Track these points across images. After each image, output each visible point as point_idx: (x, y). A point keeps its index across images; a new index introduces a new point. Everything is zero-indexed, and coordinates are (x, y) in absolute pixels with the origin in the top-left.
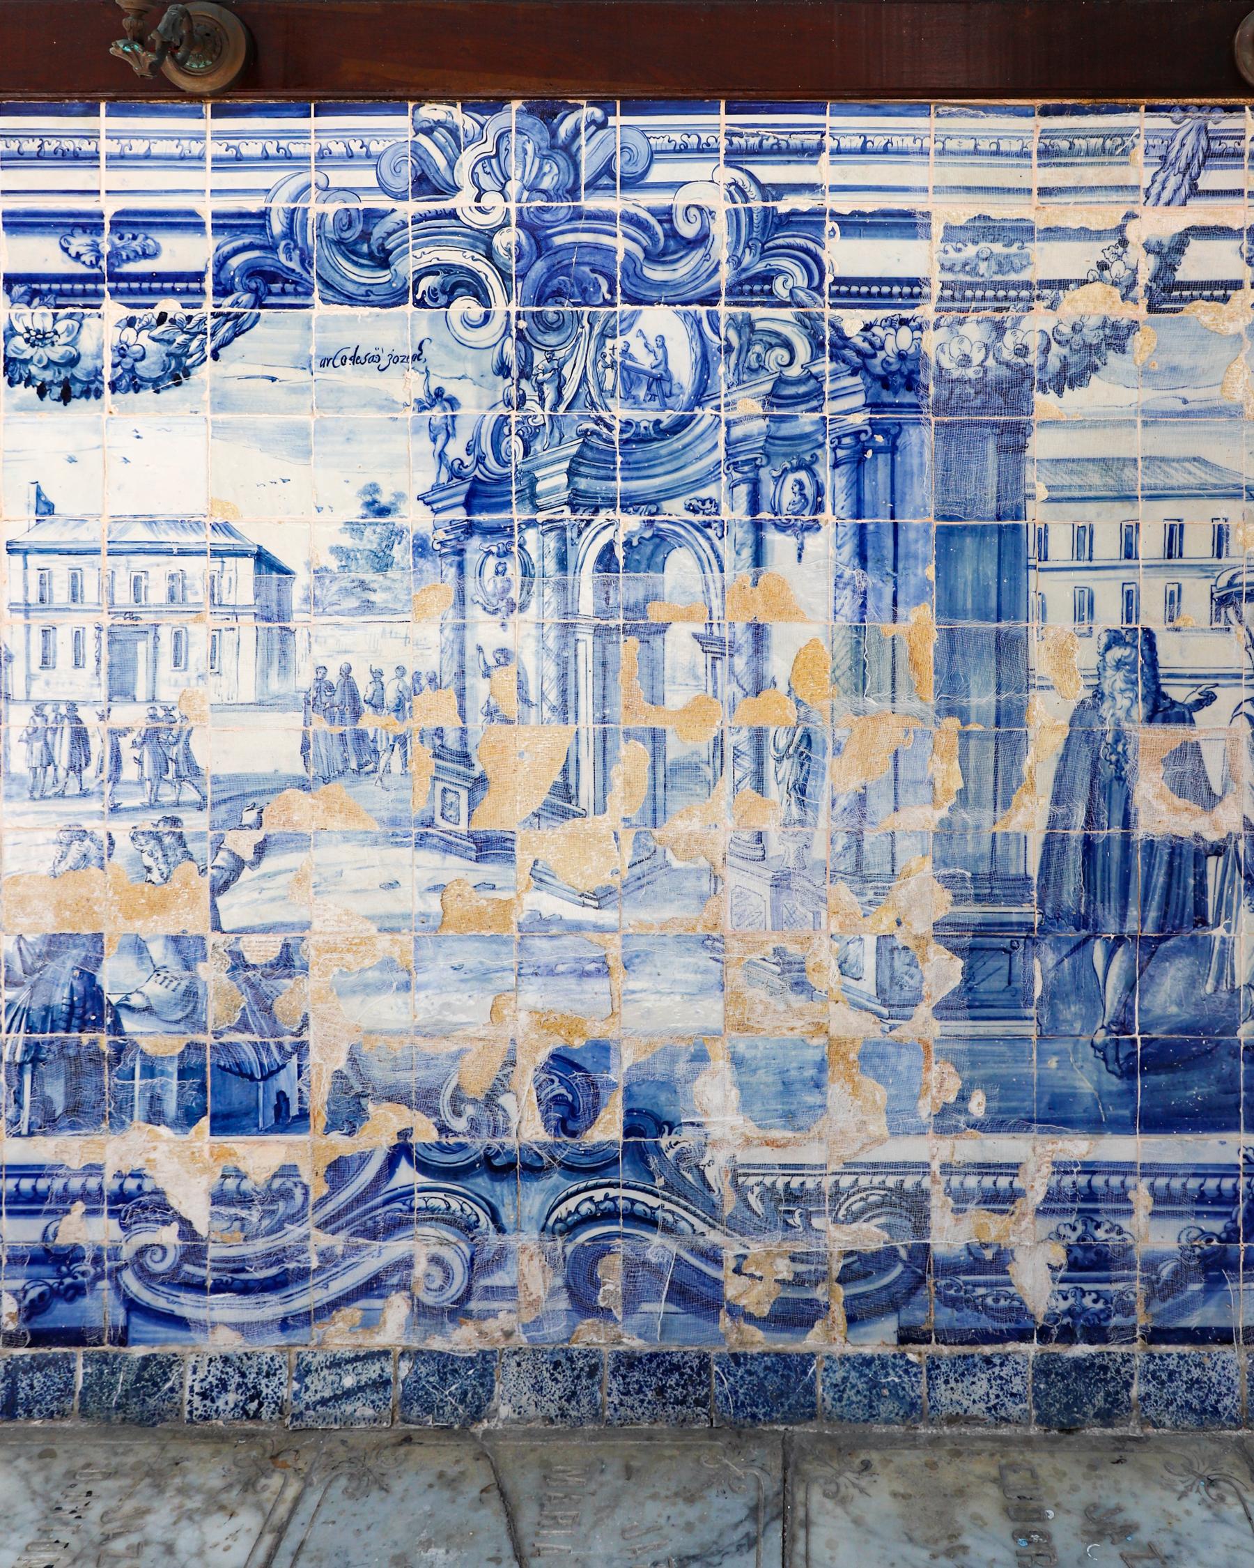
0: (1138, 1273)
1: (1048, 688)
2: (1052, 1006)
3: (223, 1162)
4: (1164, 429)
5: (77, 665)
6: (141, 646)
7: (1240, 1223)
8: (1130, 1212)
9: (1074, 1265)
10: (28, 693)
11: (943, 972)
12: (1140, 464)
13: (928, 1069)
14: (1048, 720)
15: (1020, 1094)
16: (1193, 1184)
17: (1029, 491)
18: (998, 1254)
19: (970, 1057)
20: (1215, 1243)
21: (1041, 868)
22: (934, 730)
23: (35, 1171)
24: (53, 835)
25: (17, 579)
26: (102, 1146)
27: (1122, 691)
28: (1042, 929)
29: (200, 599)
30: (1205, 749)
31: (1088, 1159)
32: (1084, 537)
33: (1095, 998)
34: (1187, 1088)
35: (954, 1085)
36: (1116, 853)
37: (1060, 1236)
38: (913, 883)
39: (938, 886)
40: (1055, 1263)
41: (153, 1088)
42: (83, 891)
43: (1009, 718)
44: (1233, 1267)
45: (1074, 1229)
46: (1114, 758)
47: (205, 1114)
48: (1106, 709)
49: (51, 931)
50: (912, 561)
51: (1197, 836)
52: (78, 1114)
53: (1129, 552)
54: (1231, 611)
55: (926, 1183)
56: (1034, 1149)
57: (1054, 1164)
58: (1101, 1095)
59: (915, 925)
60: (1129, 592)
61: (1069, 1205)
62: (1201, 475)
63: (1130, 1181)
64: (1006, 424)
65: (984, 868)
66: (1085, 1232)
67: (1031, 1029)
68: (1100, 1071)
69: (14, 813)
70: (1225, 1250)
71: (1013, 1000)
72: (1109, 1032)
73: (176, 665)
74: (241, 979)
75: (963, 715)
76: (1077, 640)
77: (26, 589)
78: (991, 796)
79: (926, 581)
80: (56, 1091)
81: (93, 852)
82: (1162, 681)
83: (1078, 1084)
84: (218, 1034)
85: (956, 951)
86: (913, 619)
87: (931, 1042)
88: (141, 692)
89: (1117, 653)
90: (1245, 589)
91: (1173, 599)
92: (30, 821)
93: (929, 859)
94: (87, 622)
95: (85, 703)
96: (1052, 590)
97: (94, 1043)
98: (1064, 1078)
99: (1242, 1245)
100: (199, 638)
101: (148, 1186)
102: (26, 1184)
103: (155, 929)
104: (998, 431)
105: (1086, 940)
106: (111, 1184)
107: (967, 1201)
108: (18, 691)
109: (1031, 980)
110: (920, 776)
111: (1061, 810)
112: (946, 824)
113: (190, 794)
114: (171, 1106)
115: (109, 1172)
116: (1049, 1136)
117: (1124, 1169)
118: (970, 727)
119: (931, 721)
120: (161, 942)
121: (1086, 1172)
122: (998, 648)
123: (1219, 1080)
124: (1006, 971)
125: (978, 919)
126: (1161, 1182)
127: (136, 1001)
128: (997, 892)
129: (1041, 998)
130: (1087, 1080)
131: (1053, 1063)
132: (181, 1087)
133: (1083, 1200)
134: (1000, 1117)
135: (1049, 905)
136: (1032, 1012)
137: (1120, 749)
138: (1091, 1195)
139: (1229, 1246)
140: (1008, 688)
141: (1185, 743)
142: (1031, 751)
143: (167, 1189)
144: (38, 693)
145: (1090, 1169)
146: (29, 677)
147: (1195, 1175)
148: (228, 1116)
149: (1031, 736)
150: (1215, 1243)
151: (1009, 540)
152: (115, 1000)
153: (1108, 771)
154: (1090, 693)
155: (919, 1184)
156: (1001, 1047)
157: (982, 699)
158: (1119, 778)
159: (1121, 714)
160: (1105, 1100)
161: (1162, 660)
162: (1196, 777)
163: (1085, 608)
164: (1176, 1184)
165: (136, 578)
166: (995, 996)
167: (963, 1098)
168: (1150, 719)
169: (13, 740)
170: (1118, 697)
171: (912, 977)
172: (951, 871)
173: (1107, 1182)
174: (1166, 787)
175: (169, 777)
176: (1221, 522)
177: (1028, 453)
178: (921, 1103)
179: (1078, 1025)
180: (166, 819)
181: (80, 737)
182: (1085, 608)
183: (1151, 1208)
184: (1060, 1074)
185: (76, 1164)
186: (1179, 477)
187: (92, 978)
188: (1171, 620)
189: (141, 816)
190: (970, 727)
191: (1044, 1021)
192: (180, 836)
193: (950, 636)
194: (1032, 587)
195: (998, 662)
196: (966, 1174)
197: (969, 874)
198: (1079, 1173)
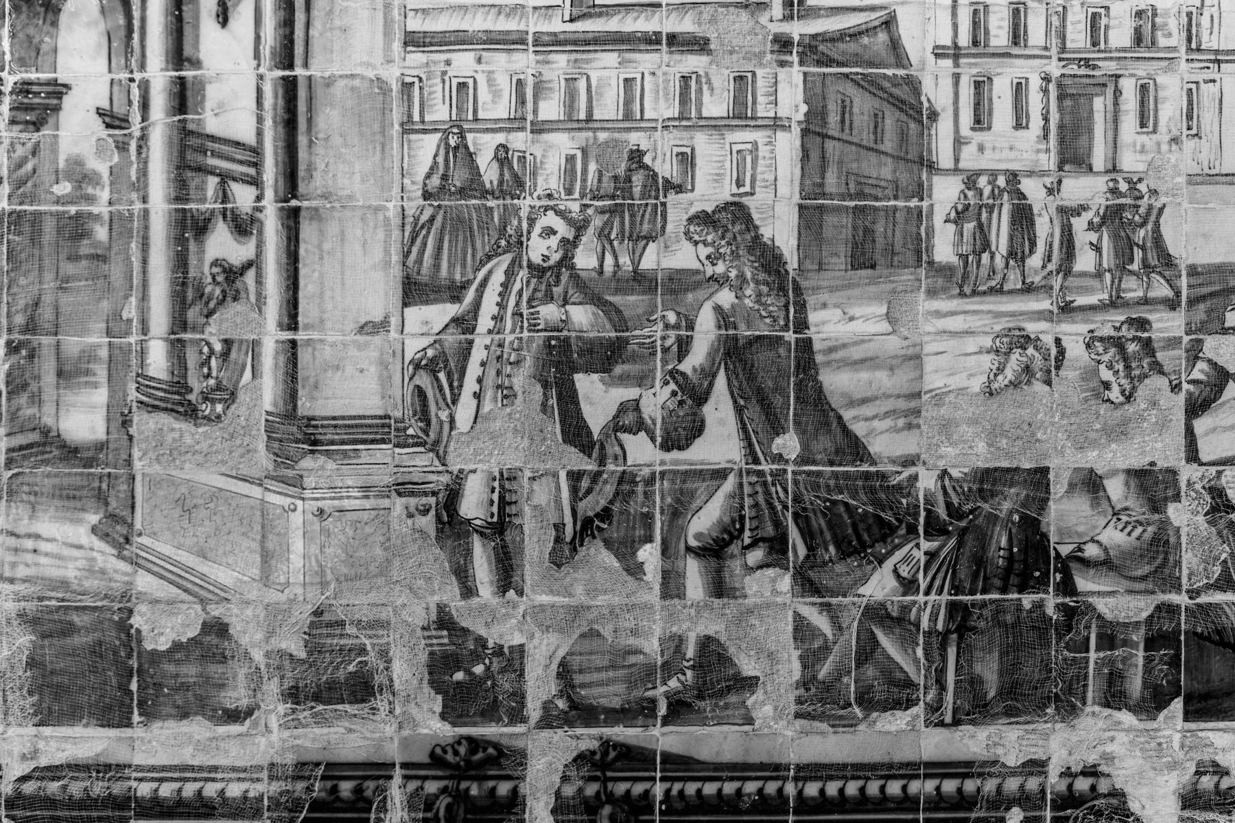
3: (1197, 756)
5: (1018, 126)
6: (1098, 103)
10: (957, 160)
23: (963, 769)
24: (987, 342)
25: (945, 19)
26: (1046, 736)
29: (1172, 42)
41: (1111, 662)
42: (1024, 413)
47: (1178, 694)
49: (981, 464)
52: (1018, 700)
69: (938, 314)
73: (1143, 125)
74: (1222, 524)
77: (955, 27)
80: (989, 670)
81: (1038, 362)
84: (1193, 593)
88: (1099, 160)
92: (956, 323)
94: (1031, 72)
95: (1031, 174)
97: (1039, 605)
100: (1171, 89)
101: (1103, 787)
102: (949, 786)
103: (1114, 459)
106: (1054, 781)
108: (944, 158)
113: (1161, 290)
114: (1135, 685)
115: (1054, 771)
120: (1121, 478)
127: (1091, 551)
132: (1148, 660)
143: (1128, 789)
144: (970, 159)
146: (959, 142)
148: (1205, 696)
152: (1065, 550)
165: (1095, 17)
169: (938, 219)
175: (1135, 267)
180: (1130, 321)
181: (1023, 217)
185: (1012, 760)
187: (1035, 523)
189: (1099, 317)
192: (1147, 345)
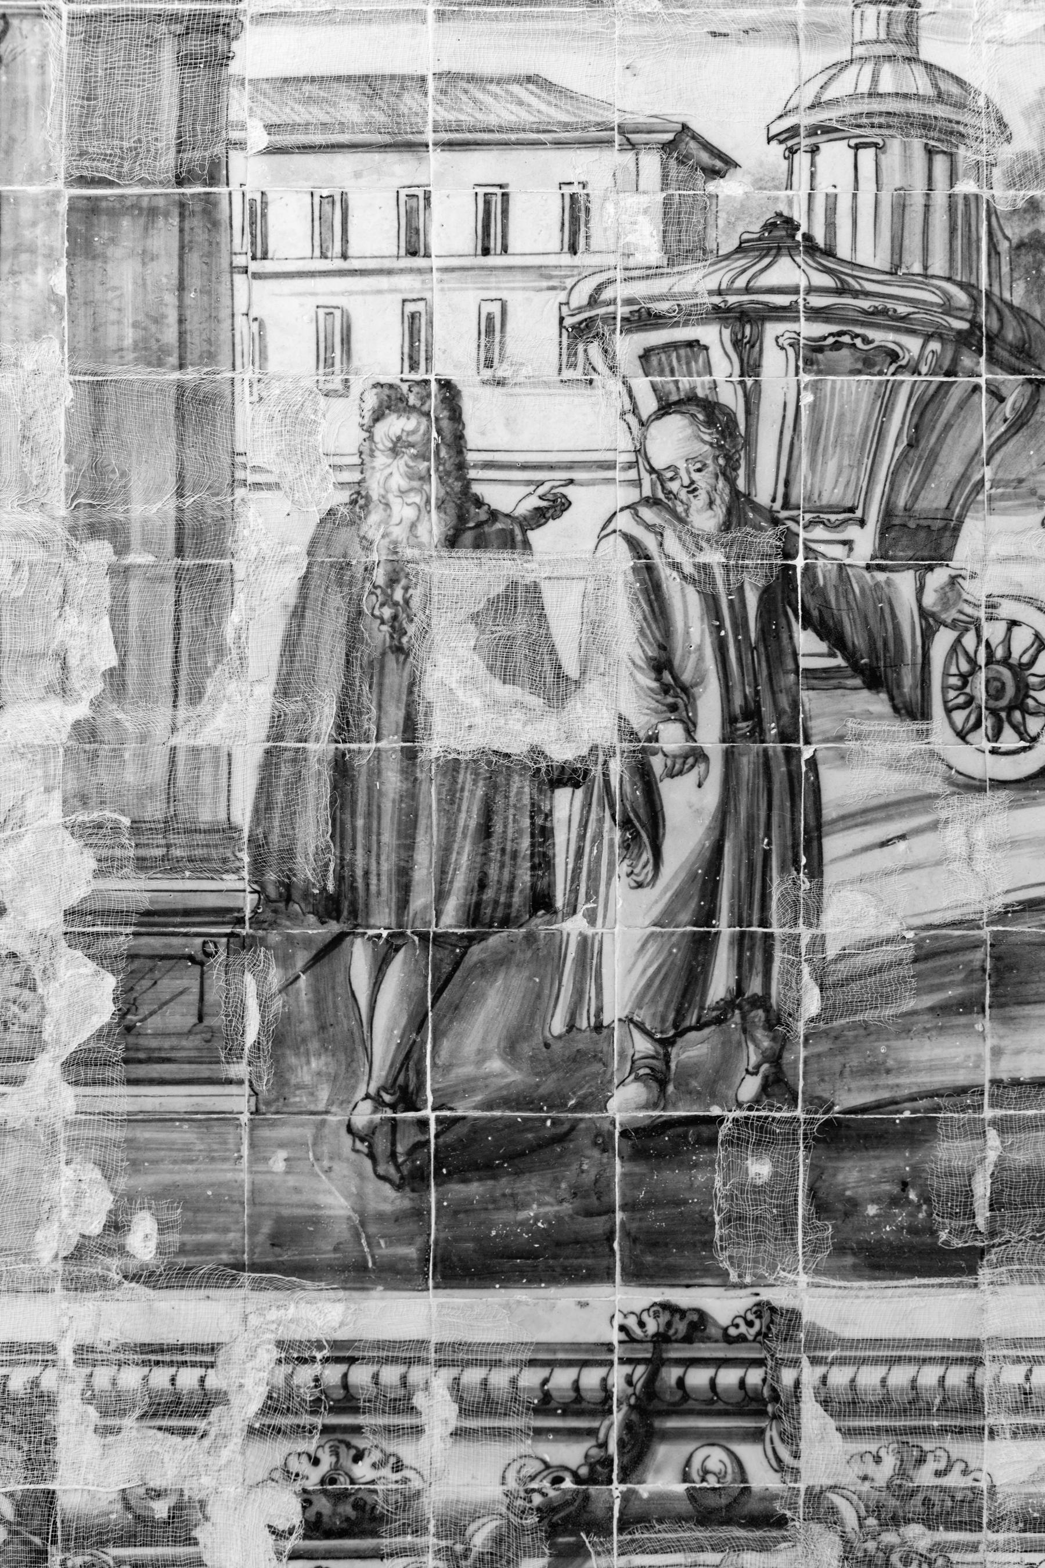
0: (430, 1540)
1: (269, 487)
2: (277, 1059)
4: (478, 26)
7: (613, 1448)
8: (417, 1431)
9: (315, 1527)
11: (81, 998)
12: (431, 85)
13: (55, 1174)
14: (270, 543)
15: (222, 1219)
16: (531, 1378)
17: (235, 135)
18: (178, 1509)
19: (125, 1152)
20: (568, 1484)
21: (256, 810)
22: (68, 565)
27: (402, 493)
28: (256, 921)
30: (549, 595)
31: (341, 1335)
32: (332, 214)
33: (354, 1045)
34: (518, 1207)
35: (100, 1204)
36: (392, 781)
37: (290, 1476)
38: (28, 842)
39: (73, 844)
40: (282, 1525)
43: (199, 541)
44: (601, 1528)
45: (316, 1462)
46: (387, 612)
48: (373, 525)
50: (24, 257)
51: (536, 752)
53: (414, 246)
54: (594, 350)
55: (49, 1380)
56: (245, 1318)
57: (280, 1344)
58: (363, 1220)
59: (32, 915)
60: (413, 316)
61: (306, 1420)
62: (542, 109)
63: (417, 1375)
64: (193, 16)
65: (155, 810)
66: (336, 1467)
67: (238, 1102)
68: (361, 1176)
70: (587, 1497)
71: (209, 1048)
72: (379, 1103)
75: (117, 535)
76: (322, 400)
78: (167, 681)
79: (53, 297)
82: (472, 474)
83: (323, 1199)
85: (101, 959)
86: (28, 364)
87: (59, 1126)
89: (395, 425)
90: (622, 311)
91: (491, 328)
93: (57, 796)
96: (280, 314)
98: (297, 1190)
99: (617, 1489)
104: (179, 28)
105: (338, 939)
107: (123, 1413)
109: (239, 1013)
110: (39, 643)
111: (293, 707)
112: (86, 732)
116: (271, 1295)
117: (407, 1353)
118: (133, 558)
119: (58, 547)
121: (338, 1360)
122: (181, 417)
123: (576, 1192)
124: (193, 997)
125: (145, 902)
126: (472, 1376)
128: (178, 853)
129: (257, 1046)
130: (338, 1192)
131: (278, 1162)
133: (332, 1410)
134: (183, 1261)
135: (271, 876)
136: (240, 1070)
137: (398, 595)
138: (347, 1401)
139: (593, 1489)
140: (196, 487)
141: (514, 585)
142: (240, 598)
145: (345, 1353)
147: (532, 1363)
149: (240, 573)
150: (568, 1484)
151: (195, 199)
153: (379, 635)
154: (345, 496)
155: (35, 1383)
156: (185, 1135)
157: (150, 506)
158: (399, 650)
159: (399, 533)
160: (372, 1229)
161: (473, 437)
162: (533, 647)
163: (337, 343)
164: (500, 1379)
166: (174, 1041)
167: (116, 1226)
168: (452, 542)
170: (396, 503)
171: (24, 1008)
172: (95, 815)
173: (376, 1377)
174: (482, 665)
176: (576, 189)
177: (234, 68)
178: (40, 1236)
179: (324, 1094)
182: (337, 343)
183: (453, 1423)
184: (292, 1181)
186: (500, 111)
188: (489, 364)
190: (133, 558)
191: (263, 1088)
193: (96, 394)
194: (240, 306)
195: (181, 439)
196: (120, 1364)
197: (126, 821)
198: (326, 1360)
